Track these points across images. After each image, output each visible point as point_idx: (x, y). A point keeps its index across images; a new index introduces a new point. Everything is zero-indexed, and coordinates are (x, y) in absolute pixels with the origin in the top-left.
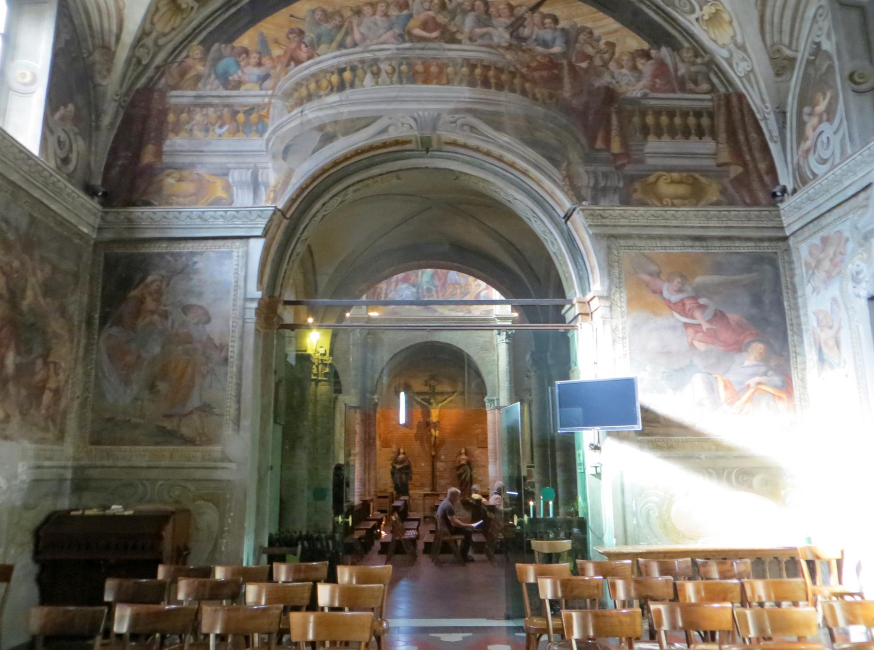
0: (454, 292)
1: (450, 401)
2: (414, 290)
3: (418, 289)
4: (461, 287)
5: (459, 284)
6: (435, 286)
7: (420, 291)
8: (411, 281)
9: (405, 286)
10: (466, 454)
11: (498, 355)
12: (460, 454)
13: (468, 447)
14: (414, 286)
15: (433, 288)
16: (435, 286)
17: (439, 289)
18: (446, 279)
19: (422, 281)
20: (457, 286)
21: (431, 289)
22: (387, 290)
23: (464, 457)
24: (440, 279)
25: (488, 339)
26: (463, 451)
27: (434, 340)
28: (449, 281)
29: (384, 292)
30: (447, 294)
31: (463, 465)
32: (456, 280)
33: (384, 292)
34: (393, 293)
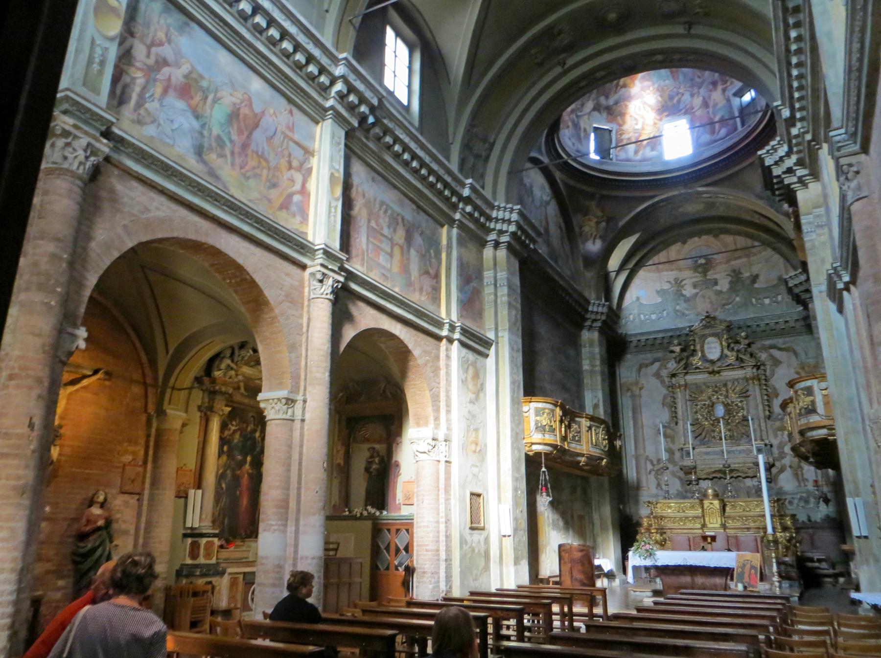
0: (258, 171)
1: (84, 388)
2: (196, 124)
3: (203, 126)
4: (269, 169)
5: (266, 160)
6: (231, 141)
7: (206, 133)
8: (193, 103)
9: (181, 105)
10: (102, 505)
11: (309, 319)
12: (91, 503)
13: (107, 491)
14: (197, 117)
15: (228, 144)
16: (231, 141)
17: (237, 150)
18: (249, 137)
19: (211, 116)
20: (264, 164)
21: (223, 141)
22: (144, 88)
23: (96, 511)
24: (240, 132)
25: (296, 284)
26: (101, 498)
27: (218, 246)
28: (253, 147)
29: (137, 89)
30: (247, 168)
31: (99, 529)
32: (263, 148)
33: (137, 89)
34: (156, 104)
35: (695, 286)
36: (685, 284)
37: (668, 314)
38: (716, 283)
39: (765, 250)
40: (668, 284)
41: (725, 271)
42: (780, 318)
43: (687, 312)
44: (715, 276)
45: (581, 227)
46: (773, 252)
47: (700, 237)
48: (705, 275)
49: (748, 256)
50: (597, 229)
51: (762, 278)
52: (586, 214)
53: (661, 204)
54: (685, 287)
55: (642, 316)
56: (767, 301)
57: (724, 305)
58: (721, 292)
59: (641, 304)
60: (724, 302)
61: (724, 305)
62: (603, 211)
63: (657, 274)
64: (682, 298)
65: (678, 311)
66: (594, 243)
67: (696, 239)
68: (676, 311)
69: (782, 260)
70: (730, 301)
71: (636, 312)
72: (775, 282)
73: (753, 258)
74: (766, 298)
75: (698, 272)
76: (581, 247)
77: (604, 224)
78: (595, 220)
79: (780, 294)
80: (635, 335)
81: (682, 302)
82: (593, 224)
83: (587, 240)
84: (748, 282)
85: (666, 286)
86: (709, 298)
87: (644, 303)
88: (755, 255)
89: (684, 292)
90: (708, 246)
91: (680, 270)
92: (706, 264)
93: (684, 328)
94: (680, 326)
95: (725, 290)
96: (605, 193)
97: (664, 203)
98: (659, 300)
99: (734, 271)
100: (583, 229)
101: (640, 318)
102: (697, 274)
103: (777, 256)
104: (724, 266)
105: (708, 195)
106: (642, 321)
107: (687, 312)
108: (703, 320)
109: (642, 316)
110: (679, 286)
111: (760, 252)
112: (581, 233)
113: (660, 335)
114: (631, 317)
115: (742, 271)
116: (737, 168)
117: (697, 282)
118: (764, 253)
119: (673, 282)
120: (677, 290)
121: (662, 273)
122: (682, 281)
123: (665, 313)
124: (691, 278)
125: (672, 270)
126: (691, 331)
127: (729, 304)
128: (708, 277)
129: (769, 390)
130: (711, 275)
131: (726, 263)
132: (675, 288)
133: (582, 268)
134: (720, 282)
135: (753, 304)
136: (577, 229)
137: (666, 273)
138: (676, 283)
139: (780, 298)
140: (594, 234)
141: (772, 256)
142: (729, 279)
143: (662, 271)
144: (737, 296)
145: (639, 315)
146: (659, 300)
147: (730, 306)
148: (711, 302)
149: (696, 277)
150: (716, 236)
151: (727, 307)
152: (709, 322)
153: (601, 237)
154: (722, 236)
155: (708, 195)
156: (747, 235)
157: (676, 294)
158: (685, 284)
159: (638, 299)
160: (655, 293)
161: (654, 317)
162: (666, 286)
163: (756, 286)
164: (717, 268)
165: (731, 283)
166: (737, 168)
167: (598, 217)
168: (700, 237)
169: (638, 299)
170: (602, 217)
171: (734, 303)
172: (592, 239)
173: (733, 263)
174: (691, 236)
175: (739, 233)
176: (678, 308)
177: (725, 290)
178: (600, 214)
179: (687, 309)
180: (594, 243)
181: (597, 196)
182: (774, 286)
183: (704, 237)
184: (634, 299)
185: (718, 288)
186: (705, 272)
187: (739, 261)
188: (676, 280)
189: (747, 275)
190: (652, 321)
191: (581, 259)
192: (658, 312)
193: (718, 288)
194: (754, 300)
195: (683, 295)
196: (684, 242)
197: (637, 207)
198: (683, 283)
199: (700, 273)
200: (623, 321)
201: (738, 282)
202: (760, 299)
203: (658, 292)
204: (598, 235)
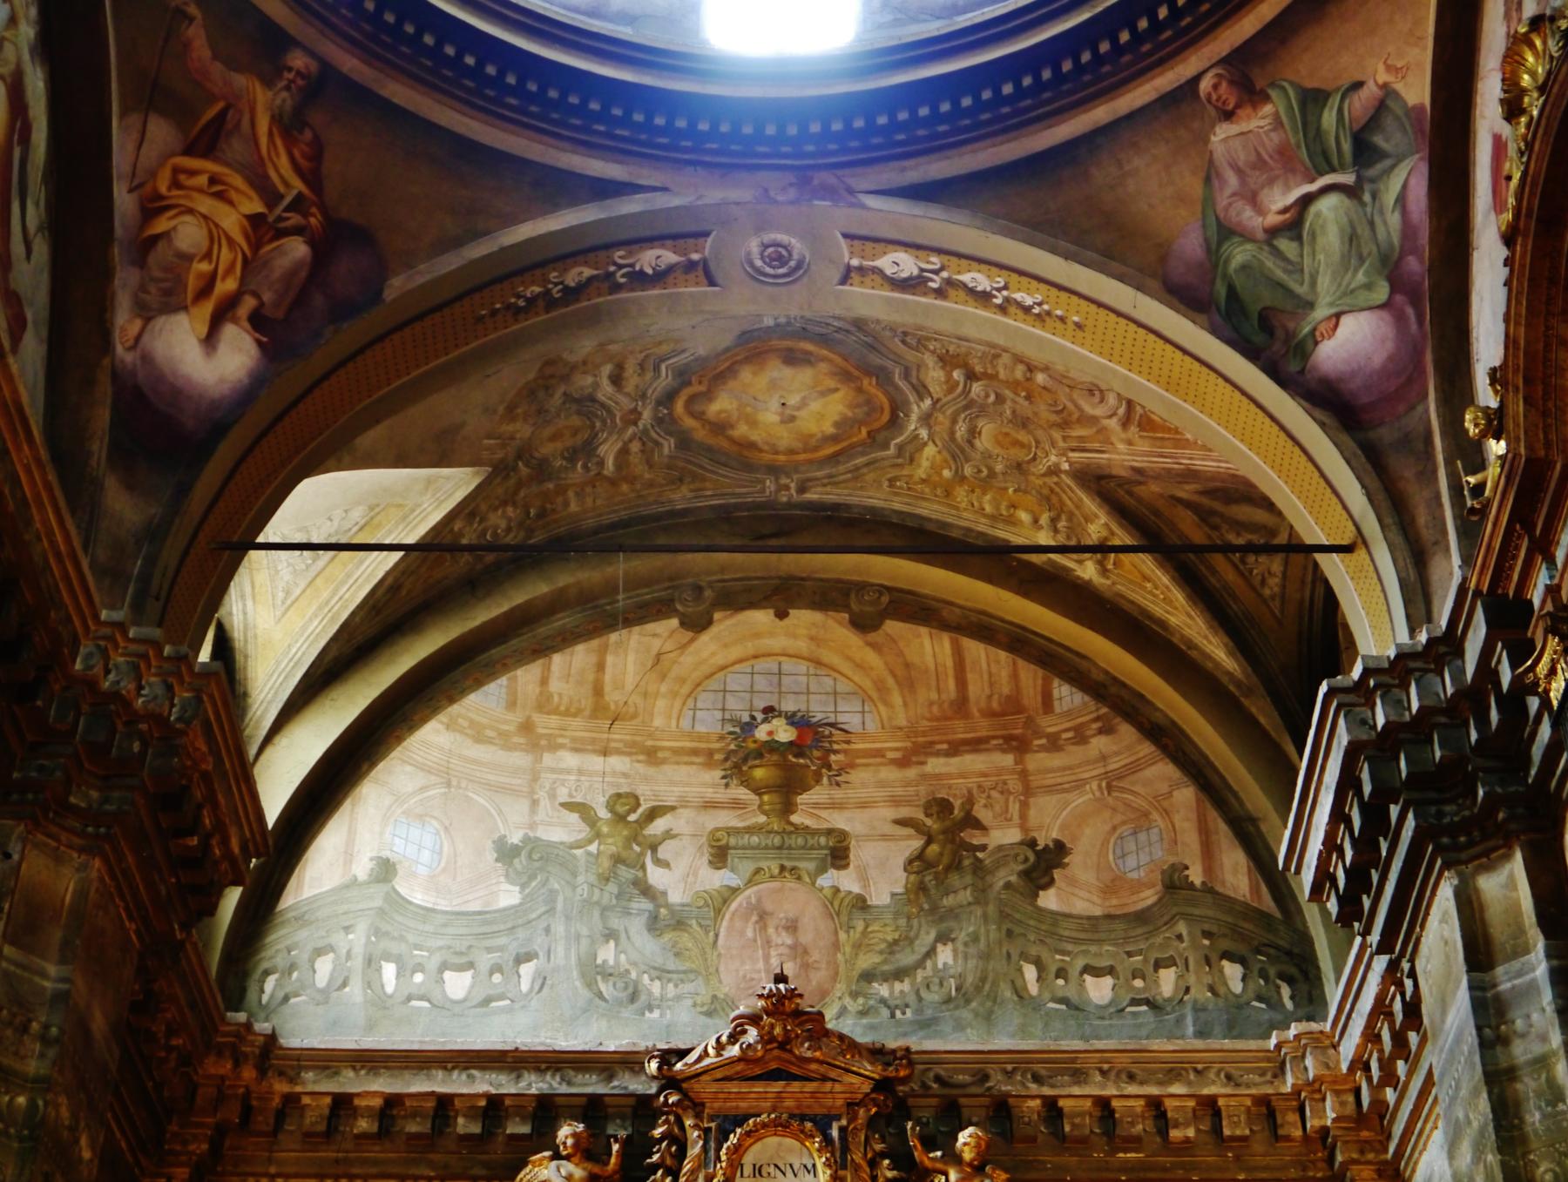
35: (720, 856)
36: (669, 835)
37: (542, 981)
38: (839, 856)
39: (1107, 730)
40: (574, 817)
41: (895, 802)
42: (1173, 1073)
43: (656, 988)
44: (839, 821)
45: (152, 207)
46: (1147, 748)
47: (782, 615)
48: (788, 808)
49: (1018, 745)
50: (250, 266)
51: (1079, 864)
52: (206, 142)
53: (650, 259)
54: (663, 852)
55: (389, 971)
56: (1099, 990)
57: (868, 977)
58: (861, 904)
59: (398, 903)
60: (866, 961)
61: (868, 977)
62: (313, 178)
63: (520, 759)
64: (645, 905)
65: (606, 974)
66: (210, 340)
67: (762, 618)
68: (593, 972)
69: (1186, 795)
70: (906, 958)
71: (357, 940)
72: (1148, 897)
73: (1037, 761)
74: (1097, 972)
75: (746, 782)
76: (124, 321)
77: (297, 249)
78: (255, 206)
79: (1170, 962)
80: (330, 1061)
81: (636, 927)
82: (230, 221)
83: (171, 300)
84: (1008, 874)
85: (562, 830)
86: (792, 927)
87: (418, 897)
88: (1054, 744)
89: (656, 876)
90: (818, 663)
91: (652, 756)
92: (796, 747)
93: (630, 1061)
94: (614, 1038)
95: (880, 896)
96: (349, 63)
97: (669, 257)
98: (509, 896)
99: (941, 807)
100: (161, 225)
101: (371, 980)
102: (743, 793)
103: (1164, 771)
104: (890, 774)
105: (903, 263)
106: (380, 1002)
107: (656, 988)
108: (754, 1019)
109: (389, 971)
110: (634, 838)
111: (1080, 737)
112: (146, 246)
113: (483, 1084)
114: (324, 966)
115: (980, 813)
116: (1100, 114)
117: (731, 831)
118: (1099, 743)
119: (604, 814)
120: (618, 860)
121: (548, 759)
122: (653, 814)
123: (527, 970)
124: (710, 805)
125: (605, 753)
126: (670, 1082)
127: (899, 974)
128: (795, 818)
129: (1461, 1115)
130: (814, 807)
131: (903, 763)
132: (612, 846)
133: (98, 448)
134: (861, 853)
135: (1020, 993)
136: (124, 201)
137: (570, 760)
138: (620, 819)
139: (1167, 981)
140: (226, 286)
141: (1133, 768)
142: (917, 843)
143: (554, 747)
144: (943, 938)
145: (371, 963)
146: (509, 896)
147: (904, 986)
148: (799, 951)
149: (736, 805)
150: (863, 624)
151: (883, 990)
152: (785, 1044)
153: (258, 322)
154: (892, 627)
155: (903, 263)
156: (1019, 642)
157: (605, 879)
158: (669, 835)
159: (386, 869)
160: (491, 856)
161: (457, 984)
162: (562, 830)
163: (1049, 900)
164: (856, 776)
165: (918, 863)
166: (1100, 114)
167: (270, 196)
168: (782, 615)
169: (386, 869)
170: (298, 204)
171: (920, 974)
172: (207, 308)
173: (935, 765)
174: (736, 598)
175: (984, 628)
176: (607, 954)
177: (880, 896)
178: (283, 171)
179: (661, 973)
180: (210, 340)
181: (298, 60)
182: (1141, 917)
183: (803, 618)
184: (362, 868)
185: (847, 881)
186: (788, 788)
187: (973, 762)
188: (621, 804)
189: (1005, 835)
190: (443, 1006)
191: (105, 389)
192: (485, 960)
193: (847, 881)
194: (1030, 972)
195: (646, 891)
196: (697, 624)
197: (513, 220)
198: (659, 826)
199: (757, 791)
200: (270, 983)
201: (955, 866)
202: (1061, 973)
203: (506, 853)
204: (249, 303)
